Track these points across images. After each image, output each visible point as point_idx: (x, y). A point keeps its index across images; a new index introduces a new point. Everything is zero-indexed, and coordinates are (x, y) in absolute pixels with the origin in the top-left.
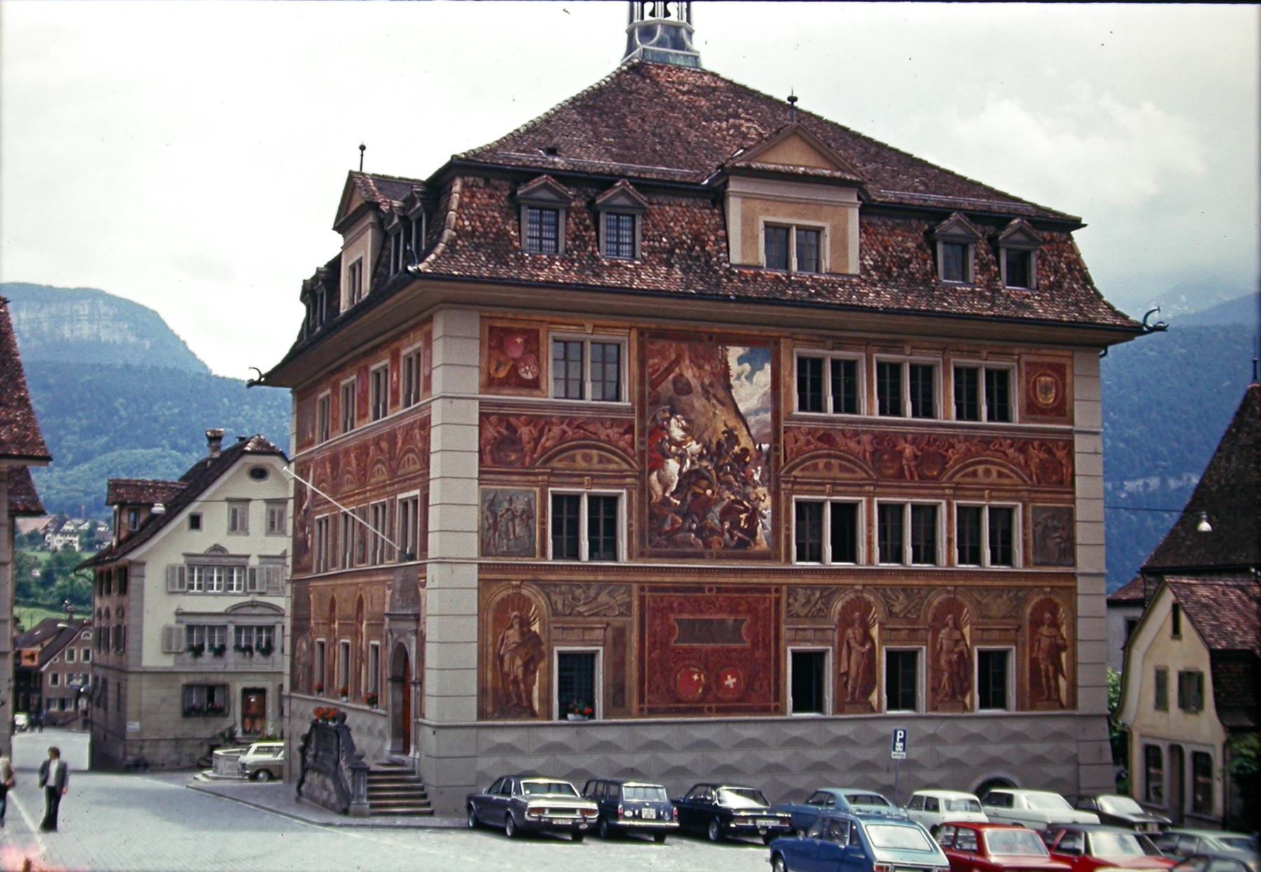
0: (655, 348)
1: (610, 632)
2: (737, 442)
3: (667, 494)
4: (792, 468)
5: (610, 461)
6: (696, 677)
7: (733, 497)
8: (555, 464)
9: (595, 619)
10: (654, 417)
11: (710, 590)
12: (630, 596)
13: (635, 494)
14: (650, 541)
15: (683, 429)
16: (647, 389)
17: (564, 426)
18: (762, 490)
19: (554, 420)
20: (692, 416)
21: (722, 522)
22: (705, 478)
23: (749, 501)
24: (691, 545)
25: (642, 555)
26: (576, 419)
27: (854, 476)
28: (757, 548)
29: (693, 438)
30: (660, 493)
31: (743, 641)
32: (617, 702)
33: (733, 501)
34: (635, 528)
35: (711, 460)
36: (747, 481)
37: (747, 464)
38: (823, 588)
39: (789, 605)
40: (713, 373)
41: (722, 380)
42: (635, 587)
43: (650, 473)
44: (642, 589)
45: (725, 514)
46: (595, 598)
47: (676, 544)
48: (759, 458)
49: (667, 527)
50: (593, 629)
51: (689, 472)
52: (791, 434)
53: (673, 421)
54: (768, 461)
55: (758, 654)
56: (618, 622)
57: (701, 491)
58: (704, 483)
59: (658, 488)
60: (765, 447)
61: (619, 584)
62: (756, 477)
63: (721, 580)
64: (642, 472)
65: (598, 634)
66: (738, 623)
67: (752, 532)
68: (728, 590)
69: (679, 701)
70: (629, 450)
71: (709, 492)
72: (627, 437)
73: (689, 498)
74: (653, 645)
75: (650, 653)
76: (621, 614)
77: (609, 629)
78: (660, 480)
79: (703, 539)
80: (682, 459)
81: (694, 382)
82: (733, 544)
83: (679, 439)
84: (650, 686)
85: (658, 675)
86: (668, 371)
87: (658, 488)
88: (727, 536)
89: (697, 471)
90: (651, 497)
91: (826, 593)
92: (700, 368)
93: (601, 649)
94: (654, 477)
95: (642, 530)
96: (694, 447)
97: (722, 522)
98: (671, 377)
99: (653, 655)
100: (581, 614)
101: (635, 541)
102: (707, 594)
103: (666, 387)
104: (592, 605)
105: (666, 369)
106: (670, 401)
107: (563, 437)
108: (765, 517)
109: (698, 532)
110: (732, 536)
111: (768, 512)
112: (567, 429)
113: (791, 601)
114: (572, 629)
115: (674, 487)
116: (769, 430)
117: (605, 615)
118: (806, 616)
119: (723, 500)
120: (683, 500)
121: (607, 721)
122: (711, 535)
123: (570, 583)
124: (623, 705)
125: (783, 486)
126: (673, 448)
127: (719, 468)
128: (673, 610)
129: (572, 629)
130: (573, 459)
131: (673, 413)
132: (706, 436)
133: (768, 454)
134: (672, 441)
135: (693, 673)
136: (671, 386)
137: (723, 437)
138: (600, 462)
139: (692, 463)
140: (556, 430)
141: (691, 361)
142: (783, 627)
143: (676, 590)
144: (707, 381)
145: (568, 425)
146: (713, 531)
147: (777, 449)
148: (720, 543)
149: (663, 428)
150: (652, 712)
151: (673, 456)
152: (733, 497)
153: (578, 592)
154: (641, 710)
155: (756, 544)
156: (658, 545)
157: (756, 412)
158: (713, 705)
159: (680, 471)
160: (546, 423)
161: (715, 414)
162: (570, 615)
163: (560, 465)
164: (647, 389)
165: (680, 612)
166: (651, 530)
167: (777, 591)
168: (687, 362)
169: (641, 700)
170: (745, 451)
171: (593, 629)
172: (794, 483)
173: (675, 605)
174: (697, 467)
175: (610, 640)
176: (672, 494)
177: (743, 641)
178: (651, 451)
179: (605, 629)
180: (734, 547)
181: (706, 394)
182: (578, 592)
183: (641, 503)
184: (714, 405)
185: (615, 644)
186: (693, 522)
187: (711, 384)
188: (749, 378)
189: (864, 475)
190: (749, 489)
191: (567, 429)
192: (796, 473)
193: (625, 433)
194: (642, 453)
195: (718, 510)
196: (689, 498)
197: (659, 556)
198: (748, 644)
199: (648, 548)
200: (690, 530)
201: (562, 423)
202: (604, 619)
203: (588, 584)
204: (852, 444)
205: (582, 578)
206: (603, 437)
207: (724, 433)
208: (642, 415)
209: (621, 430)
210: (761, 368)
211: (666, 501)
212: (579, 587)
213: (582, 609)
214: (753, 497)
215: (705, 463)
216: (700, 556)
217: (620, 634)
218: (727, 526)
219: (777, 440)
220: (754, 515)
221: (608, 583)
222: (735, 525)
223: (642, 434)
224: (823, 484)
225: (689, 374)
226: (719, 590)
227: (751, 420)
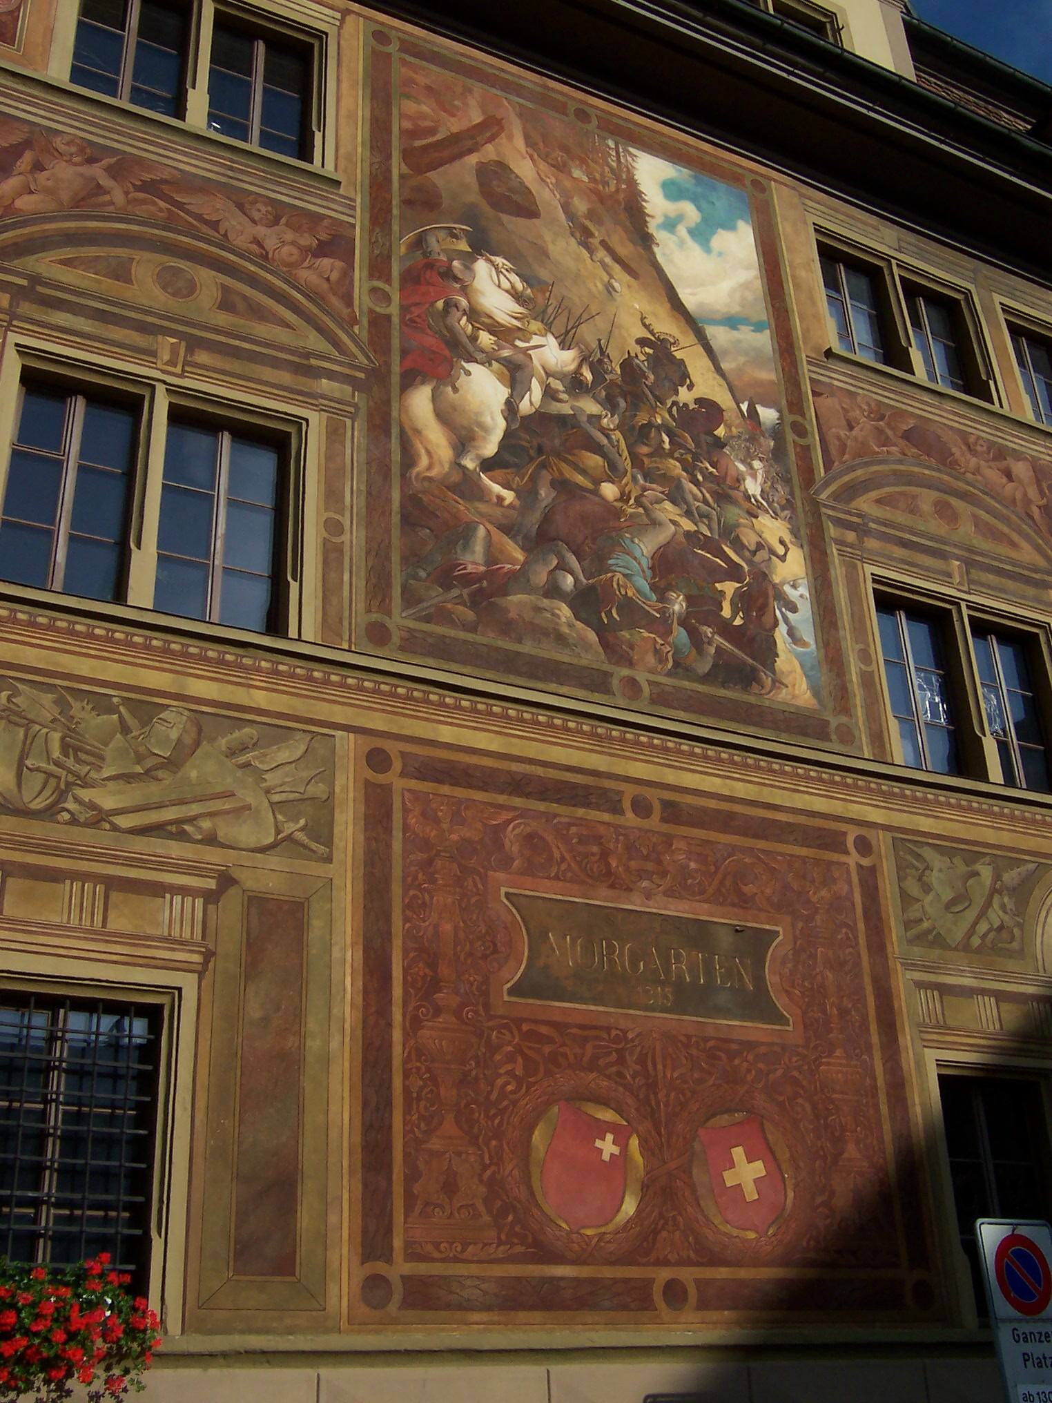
0: (422, 80)
1: (232, 907)
2: (682, 377)
3: (470, 463)
4: (851, 492)
5: (259, 313)
6: (608, 1147)
7: (687, 525)
8: (46, 265)
9: (175, 849)
10: (419, 242)
11: (642, 808)
12: (327, 774)
13: (356, 433)
14: (410, 598)
15: (517, 296)
16: (397, 167)
17: (97, 171)
18: (773, 529)
19: (58, 142)
20: (544, 274)
21: (661, 592)
22: (598, 449)
23: (738, 545)
24: (561, 639)
25: (378, 634)
26: (139, 161)
27: (1014, 555)
28: (783, 695)
29: (548, 328)
30: (444, 452)
31: (782, 1020)
32: (263, 1242)
33: (688, 534)
34: (354, 538)
35: (610, 403)
36: (725, 491)
37: (719, 444)
38: (1005, 858)
39: (906, 899)
40: (602, 199)
41: (623, 216)
42: (347, 744)
43: (410, 380)
44: (377, 759)
45: (667, 566)
46: (172, 765)
47: (507, 627)
48: (752, 439)
49: (474, 559)
50: (158, 890)
51: (541, 418)
52: (829, 402)
53: (481, 266)
54: (778, 454)
55: (836, 1068)
56: (270, 876)
57: (580, 479)
58: (594, 461)
59: (436, 439)
60: (768, 415)
61: (279, 727)
62: (753, 487)
63: (670, 777)
64: (378, 376)
65: (178, 916)
66: (755, 943)
67: (756, 645)
68: (702, 819)
69: (546, 1255)
70: (336, 302)
71: (609, 490)
72: (329, 265)
73: (545, 493)
74: (425, 988)
75: (414, 1024)
76: (283, 843)
77: (232, 903)
78: (443, 415)
79: (600, 630)
80: (515, 374)
81: (546, 197)
82: (704, 667)
83: (503, 319)
84: (412, 1176)
85: (449, 1126)
86: (458, 146)
87: (436, 439)
88: (680, 634)
89: (562, 420)
90: (409, 459)
91: (1011, 877)
92: (561, 168)
93: (188, 983)
94: (420, 401)
95: (377, 552)
96: (551, 354)
97: (661, 592)
98: (473, 159)
99: (428, 1035)
100: (99, 818)
101: (353, 582)
102: (630, 819)
103: (458, 178)
104: (153, 791)
105: (455, 138)
106: (470, 215)
107: (87, 199)
108: (794, 609)
109: (588, 602)
110: (697, 641)
111: (800, 594)
112: (105, 182)
113: (913, 889)
114: (55, 876)
115: (490, 448)
116: (768, 375)
117: (211, 840)
118: (965, 947)
119: (655, 523)
120: (527, 494)
121: (197, 1343)
122: (633, 626)
123: (71, 690)
124: (285, 1265)
125: (832, 531)
126: (485, 339)
127: (639, 434)
128: (506, 863)
129: (55, 876)
130: (121, 273)
131: (481, 246)
132: (589, 333)
133: (777, 433)
134: (474, 314)
135: (601, 1129)
136: (471, 179)
137: (642, 356)
138: (226, 304)
139: (549, 394)
140: (65, 175)
141: (529, 142)
142: (903, 980)
143: (518, 785)
144: (581, 206)
145: (113, 172)
146: (632, 612)
147: (800, 431)
148: (661, 658)
149: (449, 275)
150: (424, 1297)
151: (488, 359)
152: (687, 525)
153: (93, 723)
154: (374, 1289)
155: (777, 683)
156: (440, 615)
157: (732, 322)
158: (688, 1275)
159: (510, 408)
160: (27, 144)
161: (609, 288)
162: (49, 813)
163: (68, 276)
164: (397, 167)
165: (529, 870)
166: (413, 558)
167: (864, 846)
168: (520, 143)
169: (374, 1243)
170: (709, 411)
171: (158, 890)
172: (862, 531)
173: (512, 835)
174: (566, 409)
175: (230, 942)
176: (487, 465)
177: (782, 1020)
178: (409, 323)
179: (211, 897)
180: (705, 679)
181: (584, 236)
182: (93, 723)
183: (378, 469)
184: (604, 266)
185: (252, 965)
186: (563, 566)
187: (591, 215)
188: (702, 234)
189: (1042, 563)
190: (734, 513)
191: (105, 182)
192: (865, 504)
193: (322, 250)
194: (379, 323)
195: (646, 547)
196: (545, 493)
197: (444, 651)
198: (792, 1030)
199: (399, 619)
200: (553, 591)
201: (91, 161)
202: (214, 856)
203: (145, 705)
204: (993, 475)
205: (113, 672)
206: (241, 242)
207: (642, 342)
208: (379, 216)
209: (307, 240)
210: (730, 226)
211: (467, 487)
212: (102, 705)
213: (108, 803)
214: (749, 539)
215: (590, 406)
216: (598, 682)
217: (276, 928)
218: (678, 605)
219: (795, 405)
220: (760, 597)
221: (233, 715)
222: (703, 607)
223: (379, 268)
224: (943, 555)
225: (525, 169)
226: (672, 812)
227: (719, 336)
